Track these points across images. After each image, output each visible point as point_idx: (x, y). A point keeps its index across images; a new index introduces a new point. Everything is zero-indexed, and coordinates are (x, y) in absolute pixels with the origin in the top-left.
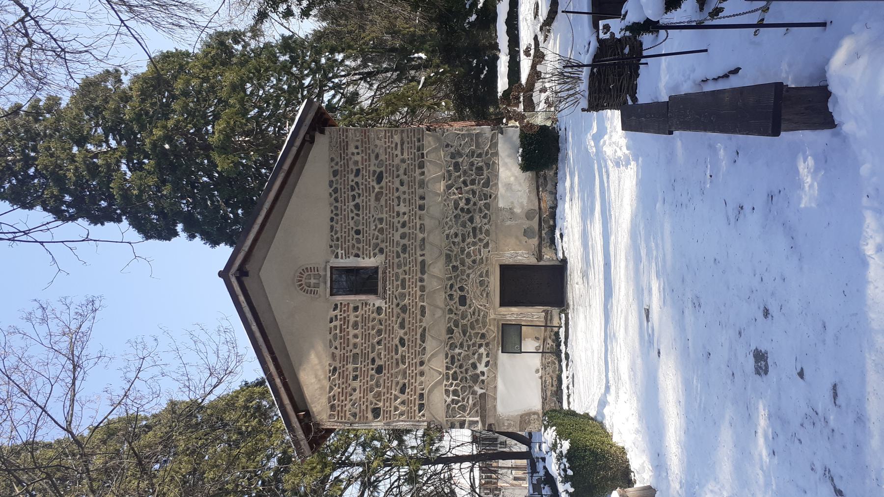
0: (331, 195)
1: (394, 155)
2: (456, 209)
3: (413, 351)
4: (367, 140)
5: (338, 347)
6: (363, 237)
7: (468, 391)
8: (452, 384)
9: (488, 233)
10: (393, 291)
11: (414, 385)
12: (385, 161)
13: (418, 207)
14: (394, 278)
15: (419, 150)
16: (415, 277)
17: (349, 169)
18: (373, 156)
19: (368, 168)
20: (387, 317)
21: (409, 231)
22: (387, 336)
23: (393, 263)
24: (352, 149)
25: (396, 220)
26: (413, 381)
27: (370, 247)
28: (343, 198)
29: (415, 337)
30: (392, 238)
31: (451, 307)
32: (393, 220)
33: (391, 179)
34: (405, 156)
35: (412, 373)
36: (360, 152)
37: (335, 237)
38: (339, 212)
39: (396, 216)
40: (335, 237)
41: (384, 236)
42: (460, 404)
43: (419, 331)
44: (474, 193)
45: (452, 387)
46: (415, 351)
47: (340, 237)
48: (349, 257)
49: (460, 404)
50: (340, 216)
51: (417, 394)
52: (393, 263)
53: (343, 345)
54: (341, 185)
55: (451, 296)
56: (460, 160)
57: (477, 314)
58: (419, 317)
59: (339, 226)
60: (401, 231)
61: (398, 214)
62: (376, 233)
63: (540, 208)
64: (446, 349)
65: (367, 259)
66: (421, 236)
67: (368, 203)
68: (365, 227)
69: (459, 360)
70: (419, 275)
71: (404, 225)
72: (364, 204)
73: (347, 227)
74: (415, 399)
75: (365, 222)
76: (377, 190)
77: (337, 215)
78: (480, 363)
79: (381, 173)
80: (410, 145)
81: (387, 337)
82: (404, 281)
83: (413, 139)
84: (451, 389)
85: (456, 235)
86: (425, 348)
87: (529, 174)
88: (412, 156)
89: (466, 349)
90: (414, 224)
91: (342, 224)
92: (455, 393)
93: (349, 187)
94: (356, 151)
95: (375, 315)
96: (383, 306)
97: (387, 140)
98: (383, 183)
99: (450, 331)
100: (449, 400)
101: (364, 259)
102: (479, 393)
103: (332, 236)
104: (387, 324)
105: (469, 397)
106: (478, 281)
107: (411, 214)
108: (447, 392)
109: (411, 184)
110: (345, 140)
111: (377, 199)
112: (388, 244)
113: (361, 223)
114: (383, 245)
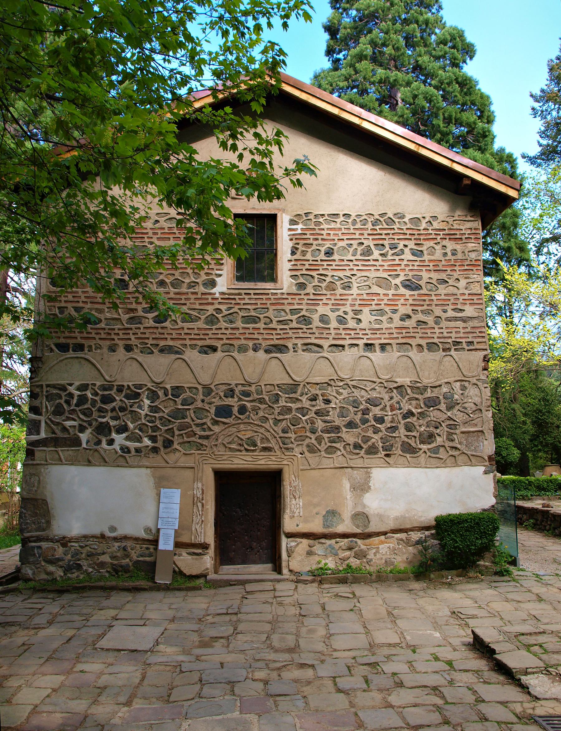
0: (382, 215)
1: (445, 308)
2: (368, 401)
3: (147, 336)
4: (466, 268)
5: (157, 225)
6: (321, 260)
7: (85, 419)
8: (96, 394)
9: (331, 450)
10: (239, 304)
11: (97, 337)
12: (436, 293)
13: (369, 342)
14: (259, 306)
15: (456, 343)
16: (260, 337)
17: (421, 242)
18: (443, 276)
19: (424, 269)
20: (199, 296)
21: (332, 329)
22: (172, 295)
23: (283, 304)
24: (450, 245)
25: (348, 309)
26: (103, 336)
27: (307, 270)
28: (379, 232)
29: (169, 337)
30: (320, 303)
32: (348, 305)
33: (411, 302)
34: (444, 324)
35: (115, 334)
36: (447, 258)
37: (321, 220)
38: (358, 226)
39: (354, 308)
40: (321, 220)
41: (324, 292)
42: (65, 406)
43: (177, 344)
44: (394, 429)
45: (92, 394)
46: (148, 338)
47: (322, 227)
48: (291, 240)
49: (65, 406)
50: (352, 227)
51: (83, 342)
52: (283, 304)
53: (159, 232)
54: (399, 229)
55: (230, 393)
56: (443, 407)
57: (203, 433)
58: (200, 343)
59: (338, 226)
60: (333, 316)
61: (357, 312)
62: (328, 279)
63: (369, 536)
64: (149, 385)
65: (289, 266)
66: (325, 344)
67: (372, 268)
68: (337, 263)
69: (131, 407)
70: (264, 344)
71: (342, 320)
72: (372, 263)
73: (336, 238)
74: (76, 338)
75: (346, 263)
76: (394, 282)
77: (354, 222)
78: (127, 438)
79: (419, 287)
80: (462, 331)
81: (170, 296)
82: (254, 320)
83: (470, 335)
84: (90, 396)
85: (328, 402)
86: (152, 353)
87: (434, 523)
88: (445, 334)
89: (148, 418)
90: (343, 336)
91: (340, 229)
92: (82, 400)
93: (396, 241)
94: (448, 250)
95: (204, 277)
96: (216, 290)
97: (466, 297)
98: (402, 291)
99: (177, 390)
100: (71, 389)
101: (290, 261)
102: (81, 435)
103: (323, 215)
104: (190, 296)
105: (75, 420)
107: (358, 331)
108: (83, 387)
109: (404, 331)
110: (463, 237)
111: (382, 282)
112: (312, 297)
113: (342, 258)
114: (310, 289)
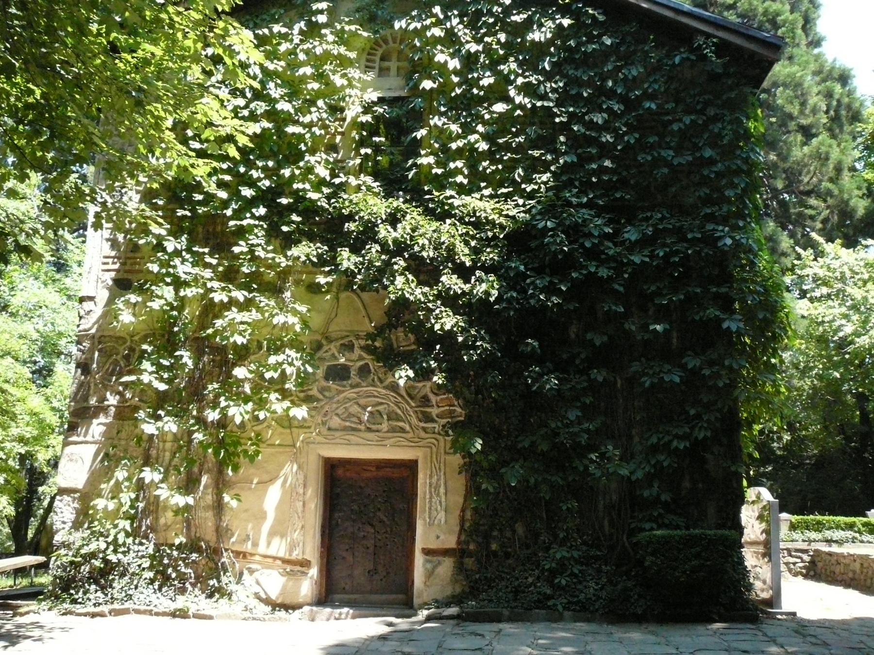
31: (325, 348)
106: (380, 408)
